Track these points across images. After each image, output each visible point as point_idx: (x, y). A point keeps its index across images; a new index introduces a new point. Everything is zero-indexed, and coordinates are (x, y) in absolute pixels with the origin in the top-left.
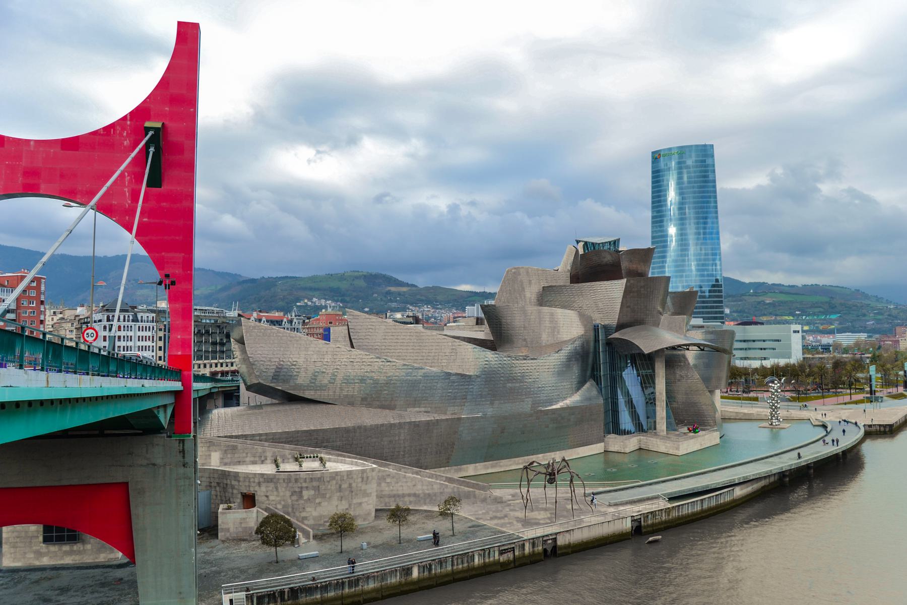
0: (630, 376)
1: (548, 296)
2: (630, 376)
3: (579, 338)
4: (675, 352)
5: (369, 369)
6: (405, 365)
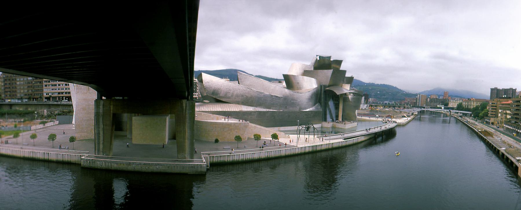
0: (331, 104)
1: (306, 73)
5: (245, 92)
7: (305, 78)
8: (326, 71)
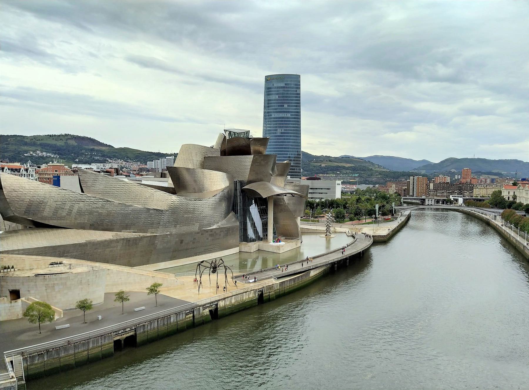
1: (209, 162)
2: (254, 210)
3: (226, 188)
4: (278, 197)
5: (95, 206)
6: (119, 204)
7: (206, 171)
8: (241, 156)
